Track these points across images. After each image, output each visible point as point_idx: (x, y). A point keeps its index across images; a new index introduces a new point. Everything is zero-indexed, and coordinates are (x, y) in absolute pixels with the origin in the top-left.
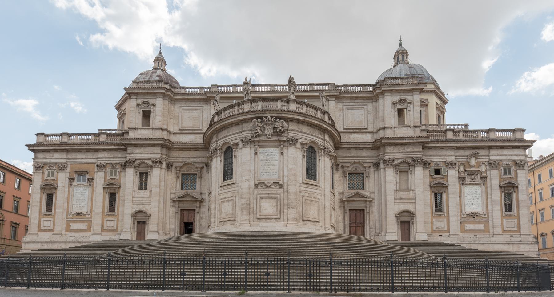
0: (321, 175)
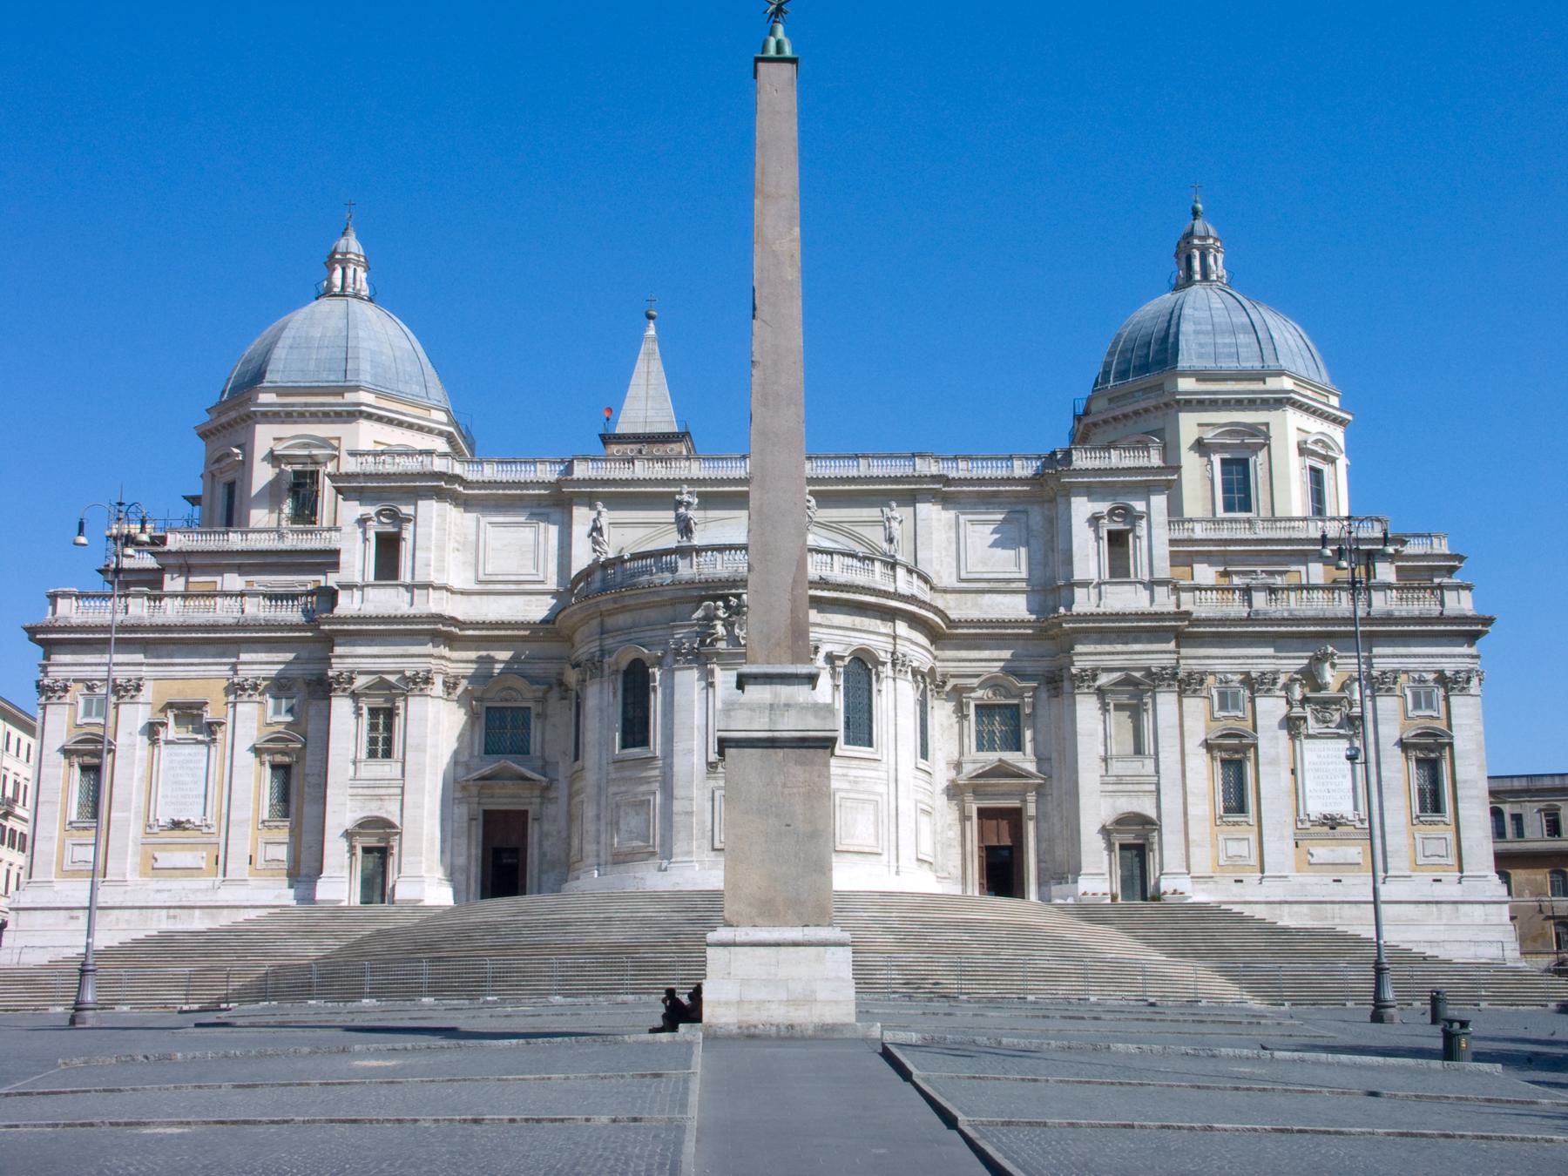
0: (885, 728)
